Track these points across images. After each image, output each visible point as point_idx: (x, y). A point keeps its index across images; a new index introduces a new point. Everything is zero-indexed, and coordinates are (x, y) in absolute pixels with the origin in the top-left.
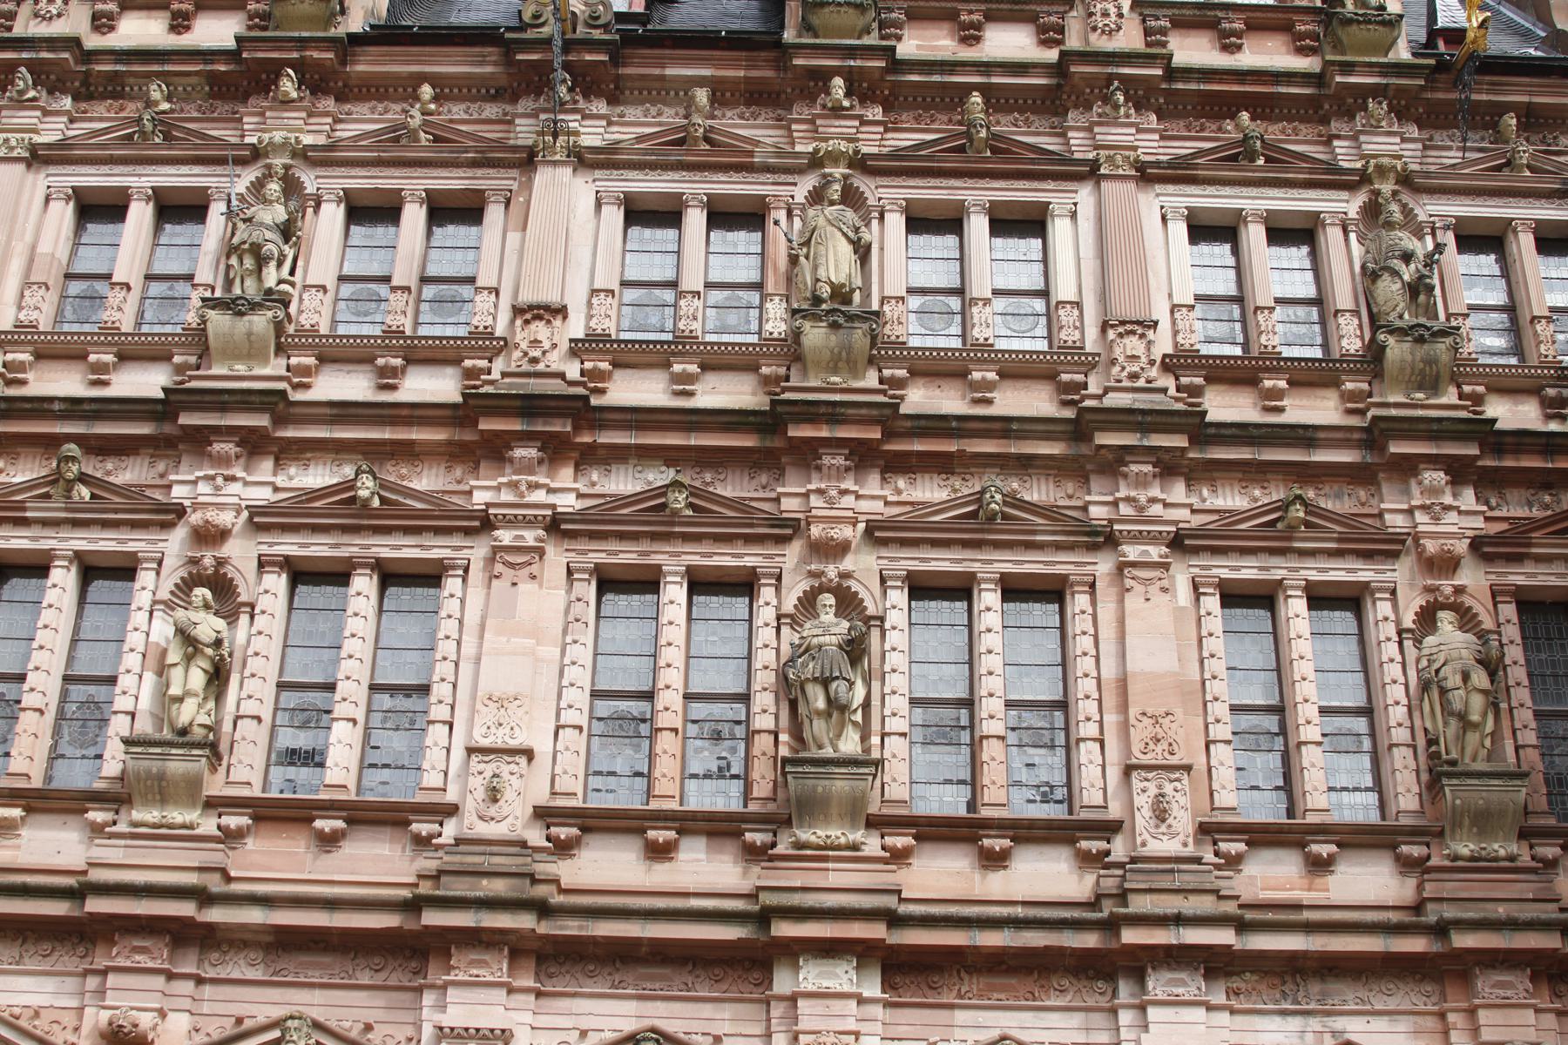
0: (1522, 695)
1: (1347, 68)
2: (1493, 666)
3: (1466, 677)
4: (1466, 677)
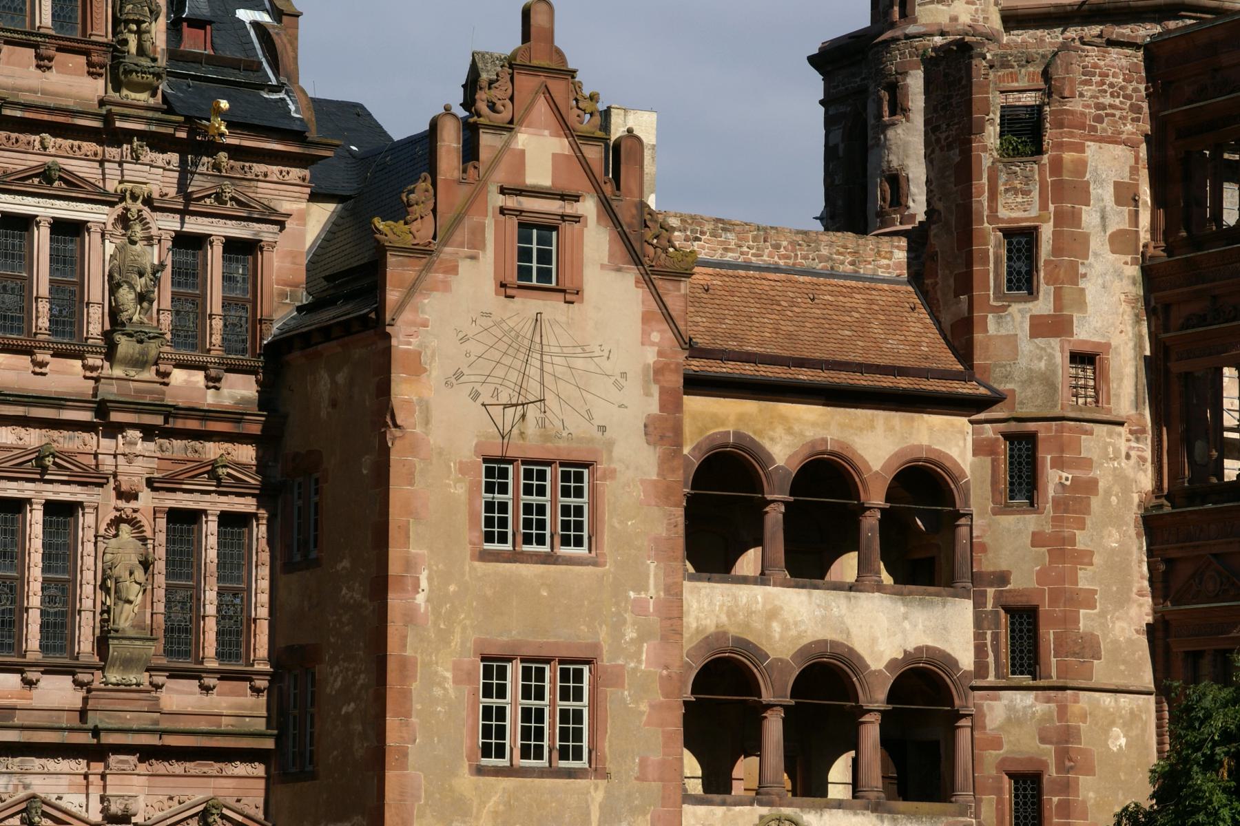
0: (161, 580)
1: (125, 117)
2: (146, 564)
3: (131, 574)
4: (131, 574)
